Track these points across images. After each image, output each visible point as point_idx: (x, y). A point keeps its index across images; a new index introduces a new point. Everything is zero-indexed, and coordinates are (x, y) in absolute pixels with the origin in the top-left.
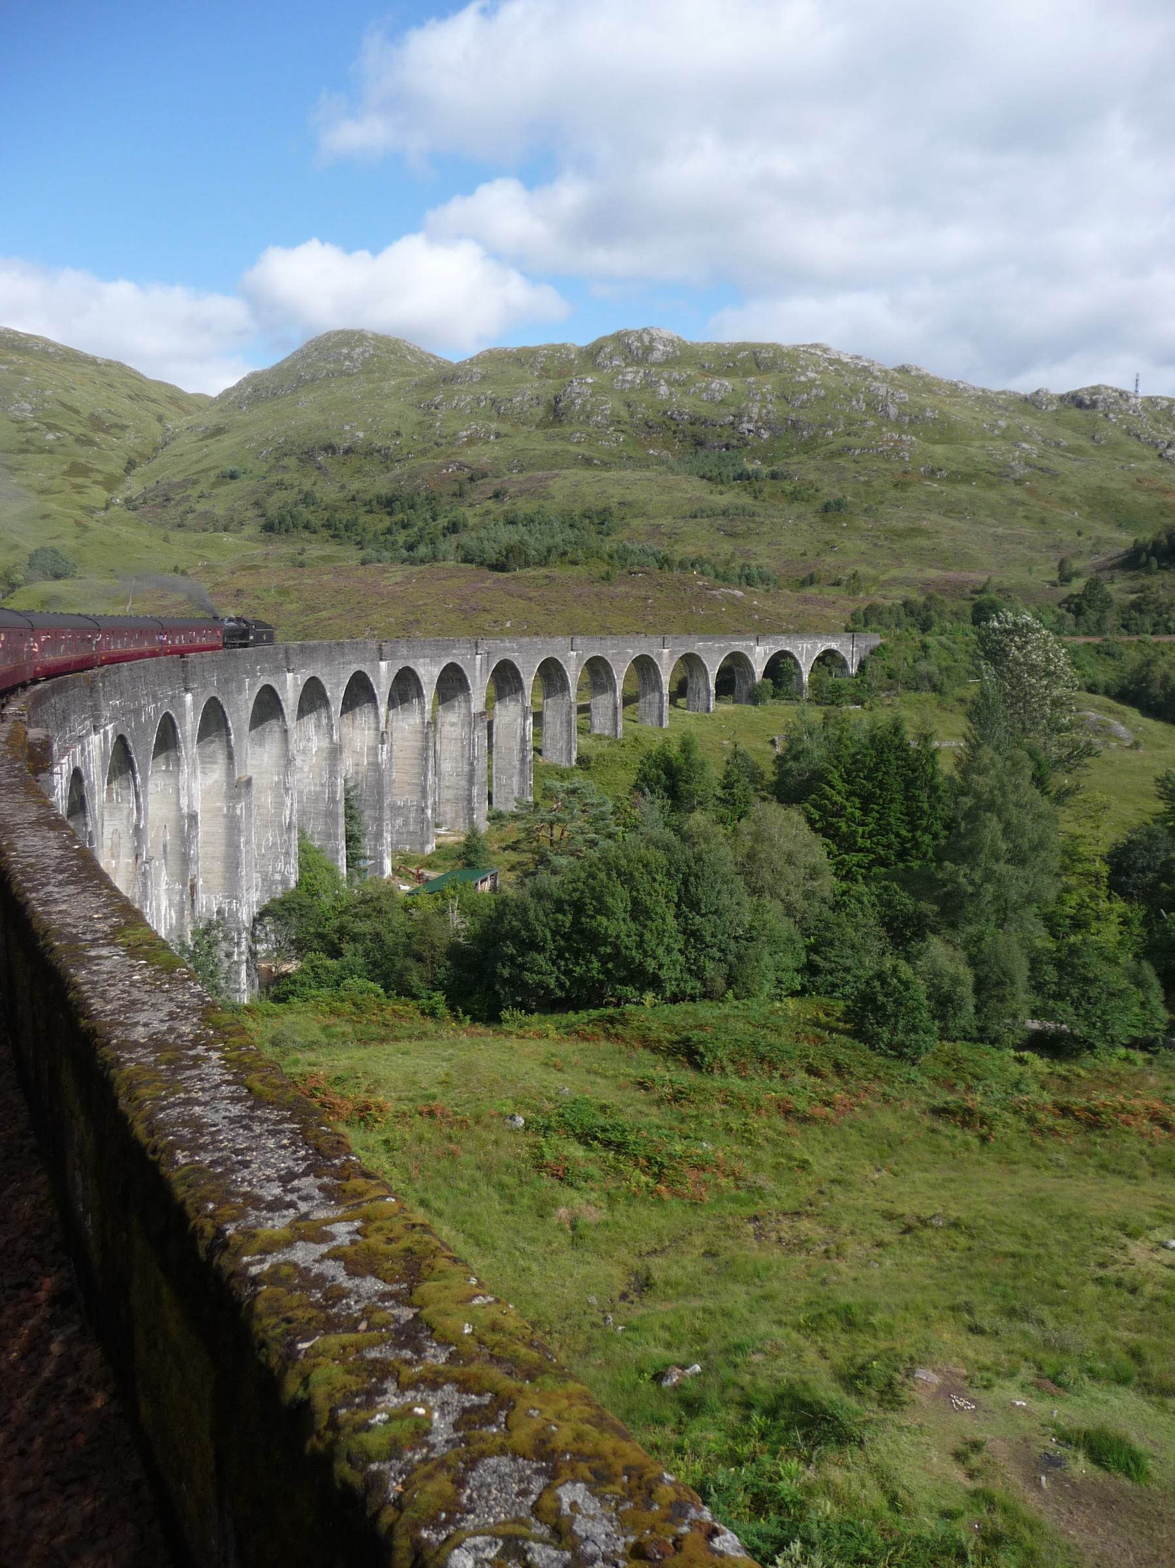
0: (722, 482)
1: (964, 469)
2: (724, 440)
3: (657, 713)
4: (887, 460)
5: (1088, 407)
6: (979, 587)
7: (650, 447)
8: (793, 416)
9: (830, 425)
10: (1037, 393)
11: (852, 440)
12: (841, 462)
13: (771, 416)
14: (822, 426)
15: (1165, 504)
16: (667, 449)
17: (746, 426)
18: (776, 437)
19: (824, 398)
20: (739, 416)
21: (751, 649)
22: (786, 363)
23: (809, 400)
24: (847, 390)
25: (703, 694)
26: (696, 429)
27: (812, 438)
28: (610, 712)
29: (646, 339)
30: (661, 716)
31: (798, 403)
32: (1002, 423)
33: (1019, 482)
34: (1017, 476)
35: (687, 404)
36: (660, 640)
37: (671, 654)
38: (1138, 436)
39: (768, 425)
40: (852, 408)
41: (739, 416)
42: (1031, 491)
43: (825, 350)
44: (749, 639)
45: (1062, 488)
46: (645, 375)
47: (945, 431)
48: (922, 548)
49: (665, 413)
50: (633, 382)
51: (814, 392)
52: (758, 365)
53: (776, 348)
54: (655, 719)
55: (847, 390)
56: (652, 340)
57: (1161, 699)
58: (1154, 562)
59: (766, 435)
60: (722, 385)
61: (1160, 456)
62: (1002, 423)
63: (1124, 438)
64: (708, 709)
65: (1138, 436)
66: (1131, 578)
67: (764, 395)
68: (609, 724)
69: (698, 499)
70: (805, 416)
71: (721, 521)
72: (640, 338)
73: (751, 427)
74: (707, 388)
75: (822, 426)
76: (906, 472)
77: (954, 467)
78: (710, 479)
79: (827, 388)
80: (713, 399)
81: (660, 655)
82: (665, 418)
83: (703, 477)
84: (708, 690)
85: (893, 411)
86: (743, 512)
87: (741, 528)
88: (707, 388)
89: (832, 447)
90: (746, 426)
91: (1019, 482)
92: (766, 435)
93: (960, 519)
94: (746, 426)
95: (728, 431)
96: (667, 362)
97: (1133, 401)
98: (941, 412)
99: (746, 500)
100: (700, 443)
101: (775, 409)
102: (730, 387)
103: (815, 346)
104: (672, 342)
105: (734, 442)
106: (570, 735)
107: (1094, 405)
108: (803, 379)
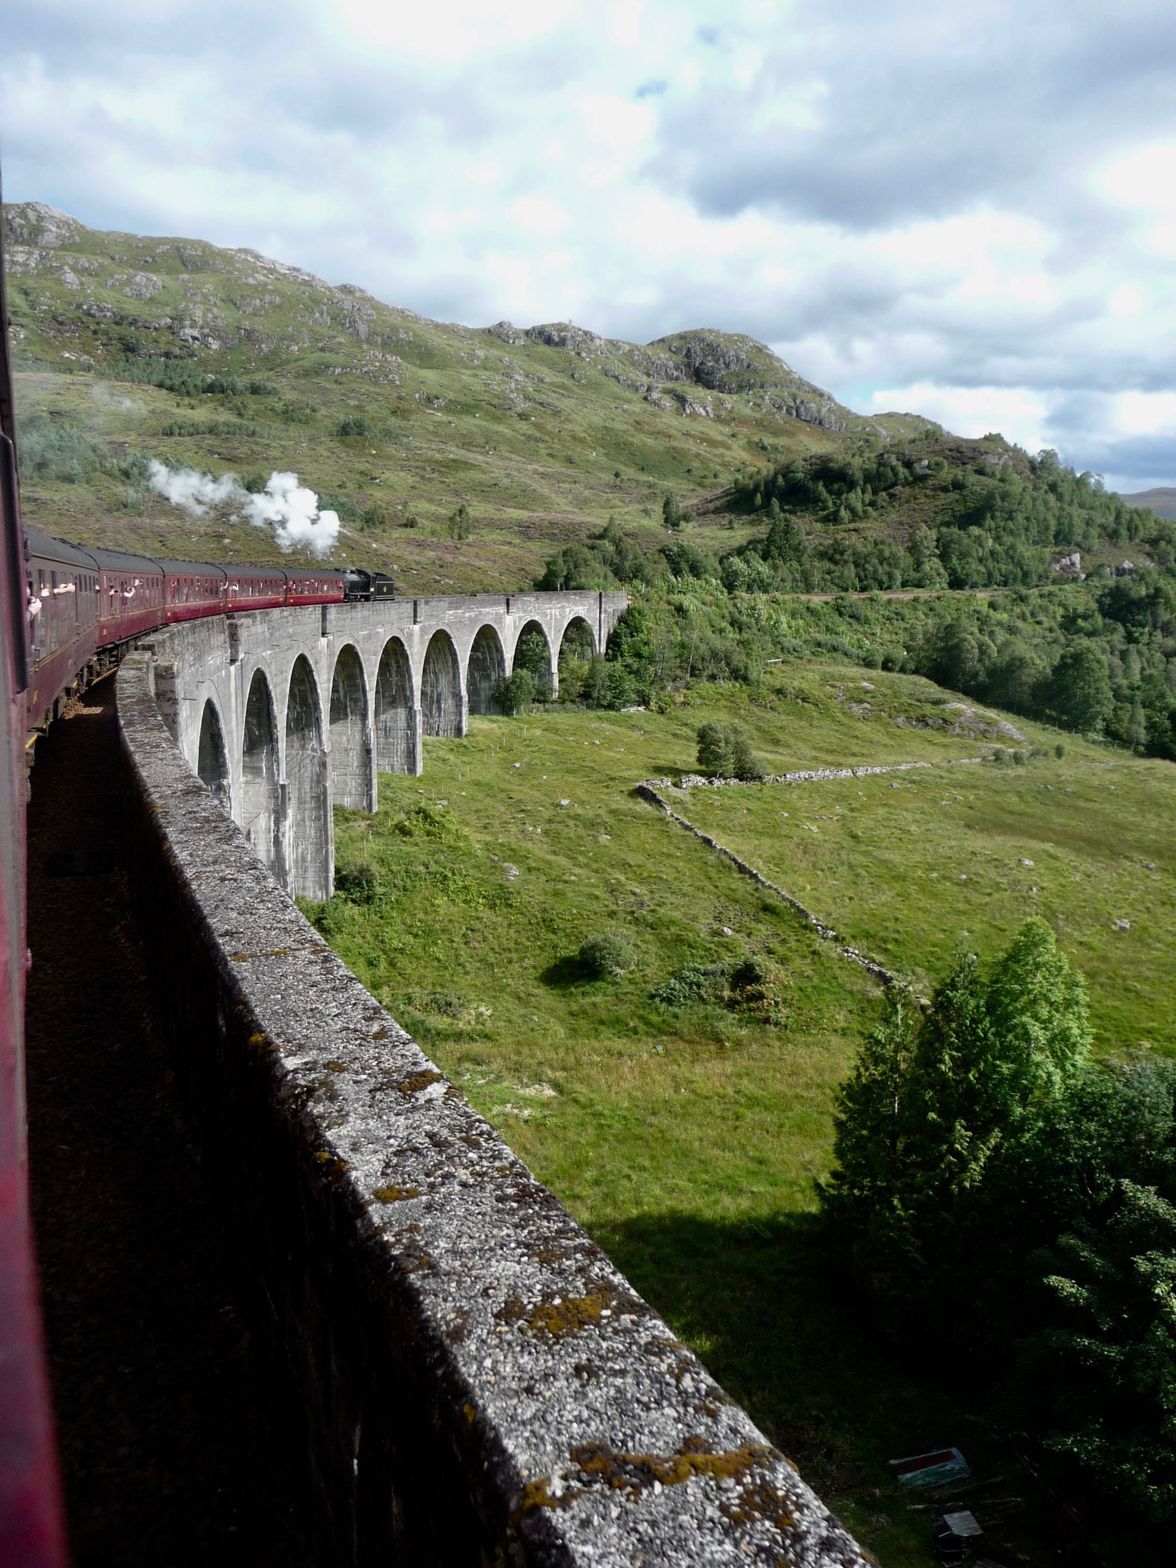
0: (188, 394)
1: (463, 399)
2: (163, 348)
3: (402, 746)
4: (376, 384)
5: (557, 344)
6: (598, 531)
7: (65, 347)
8: (247, 324)
9: (292, 339)
10: (501, 325)
11: (328, 357)
12: (321, 381)
13: (220, 322)
14: (282, 339)
15: (674, 448)
16: (89, 353)
17: (188, 331)
18: (227, 348)
19: (280, 307)
20: (178, 318)
21: (499, 618)
22: (219, 263)
23: (263, 307)
24: (306, 300)
25: (448, 704)
26: (124, 330)
27: (275, 352)
28: (354, 759)
29: (32, 215)
30: (411, 754)
31: (249, 310)
32: (481, 353)
33: (523, 417)
34: (519, 410)
35: (108, 298)
36: (410, 606)
37: (422, 630)
38: (616, 378)
39: (217, 333)
40: (315, 321)
41: (178, 318)
42: (537, 426)
43: (258, 257)
44: (495, 603)
45: (569, 426)
46: (42, 258)
47: (425, 355)
48: (480, 484)
49: (79, 306)
50: (25, 265)
51: (267, 298)
52: (184, 263)
53: (205, 246)
54: (399, 761)
55: (306, 300)
56: (40, 218)
57: (982, 677)
58: (775, 502)
59: (215, 345)
60: (151, 281)
61: (645, 399)
62: (481, 353)
63: (603, 378)
64: (459, 731)
65: (616, 378)
66: (752, 523)
67: (204, 296)
68: (353, 783)
69: (165, 412)
70: (261, 325)
71: (210, 441)
72: (23, 214)
73: (196, 333)
74: (128, 282)
75: (282, 339)
76: (400, 398)
77: (451, 396)
78: (171, 389)
79: (283, 295)
80: (139, 296)
81: (410, 635)
82: (79, 313)
83: (160, 386)
84: (457, 696)
85: (363, 329)
86: (233, 431)
87: (243, 451)
88: (128, 282)
89: (306, 363)
90: (189, 332)
91: (523, 417)
92: (215, 345)
93: (481, 453)
94: (188, 331)
95: (165, 337)
96: (63, 247)
97: (598, 342)
98: (415, 334)
99: (225, 416)
100: (130, 349)
101: (224, 316)
102: (160, 284)
103: (246, 251)
104: (67, 223)
105: (177, 351)
106: (324, 829)
107: (563, 342)
108: (251, 281)
